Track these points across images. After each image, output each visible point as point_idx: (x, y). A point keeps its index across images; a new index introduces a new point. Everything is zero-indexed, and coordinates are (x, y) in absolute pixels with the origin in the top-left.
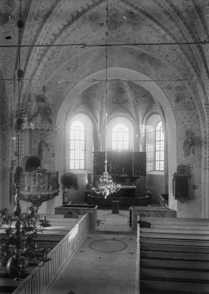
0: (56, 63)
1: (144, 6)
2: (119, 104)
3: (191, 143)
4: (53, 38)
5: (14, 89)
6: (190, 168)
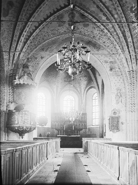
0: (35, 45)
1: (91, 11)
3: (119, 95)
4: (34, 28)
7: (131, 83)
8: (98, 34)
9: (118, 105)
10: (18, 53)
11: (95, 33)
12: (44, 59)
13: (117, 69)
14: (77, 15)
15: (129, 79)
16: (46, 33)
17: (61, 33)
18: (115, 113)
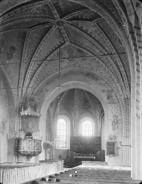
2: (86, 109)
5: (18, 94)
6: (115, 137)
7: (126, 110)
8: (95, 65)
9: (115, 131)
10: (25, 89)
11: (92, 65)
12: (48, 92)
13: (114, 97)
14: (75, 51)
15: (124, 106)
16: (49, 69)
17: (62, 68)
18: (111, 139)
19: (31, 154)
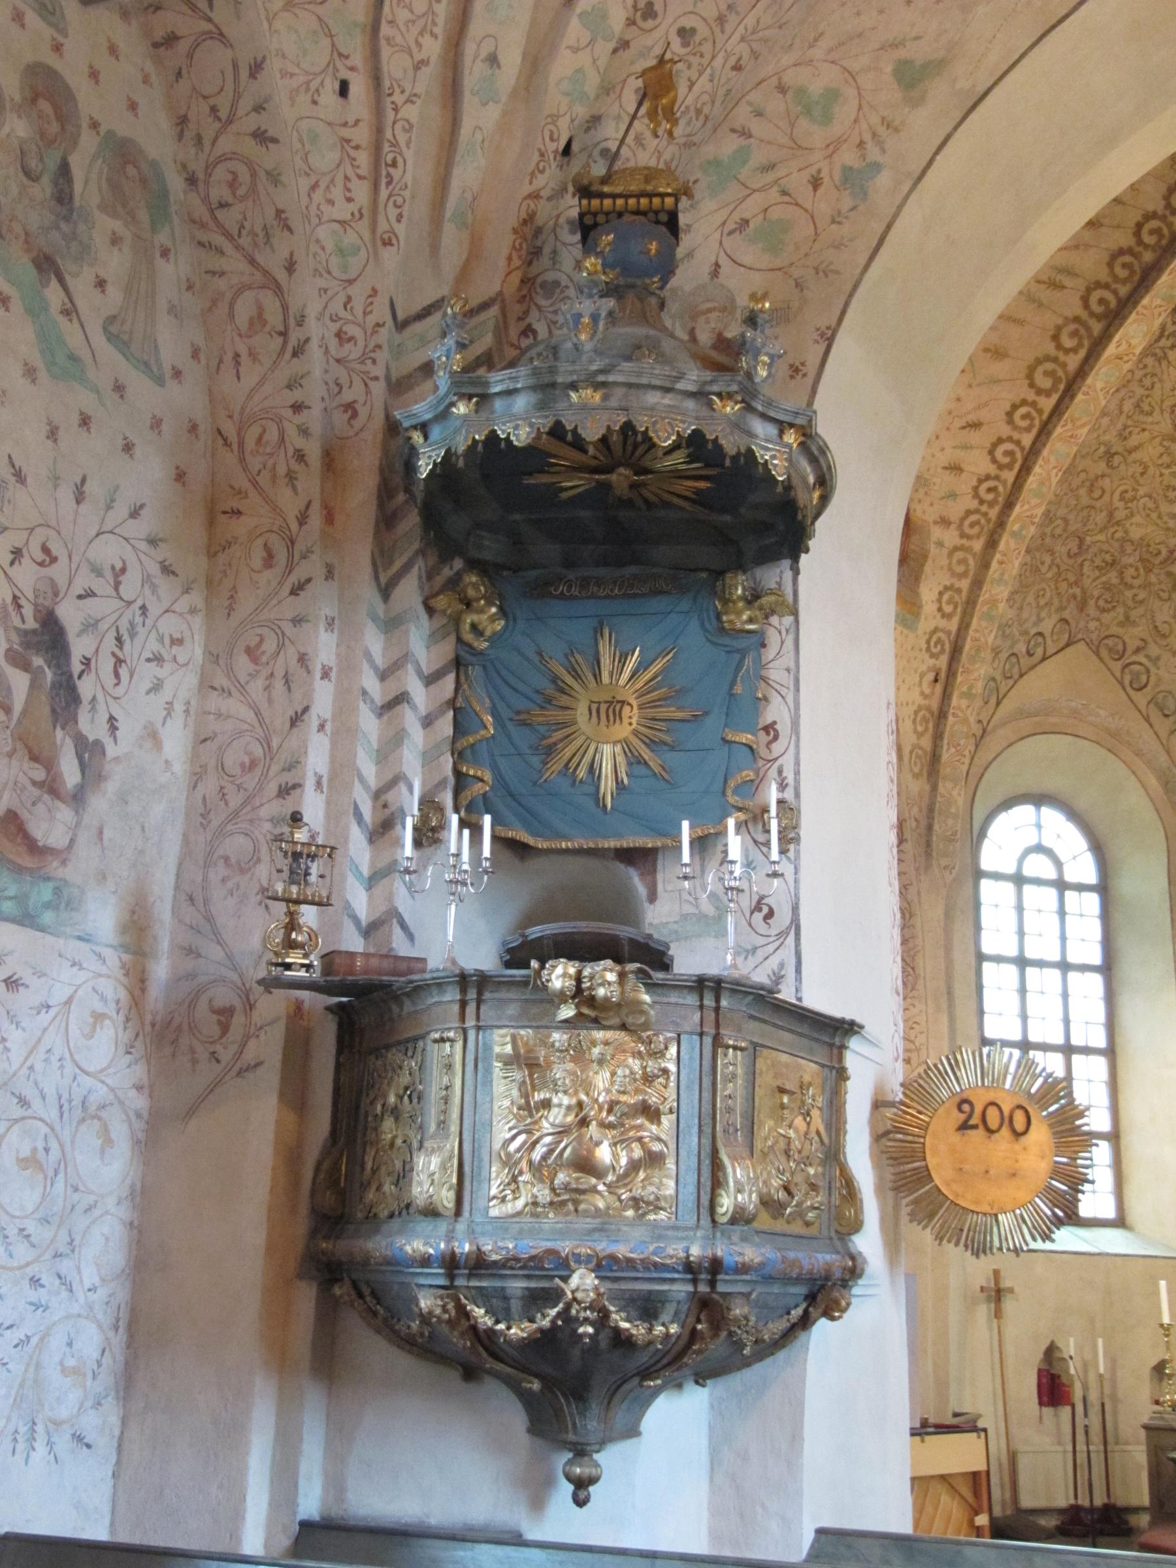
19: (621, 1341)
